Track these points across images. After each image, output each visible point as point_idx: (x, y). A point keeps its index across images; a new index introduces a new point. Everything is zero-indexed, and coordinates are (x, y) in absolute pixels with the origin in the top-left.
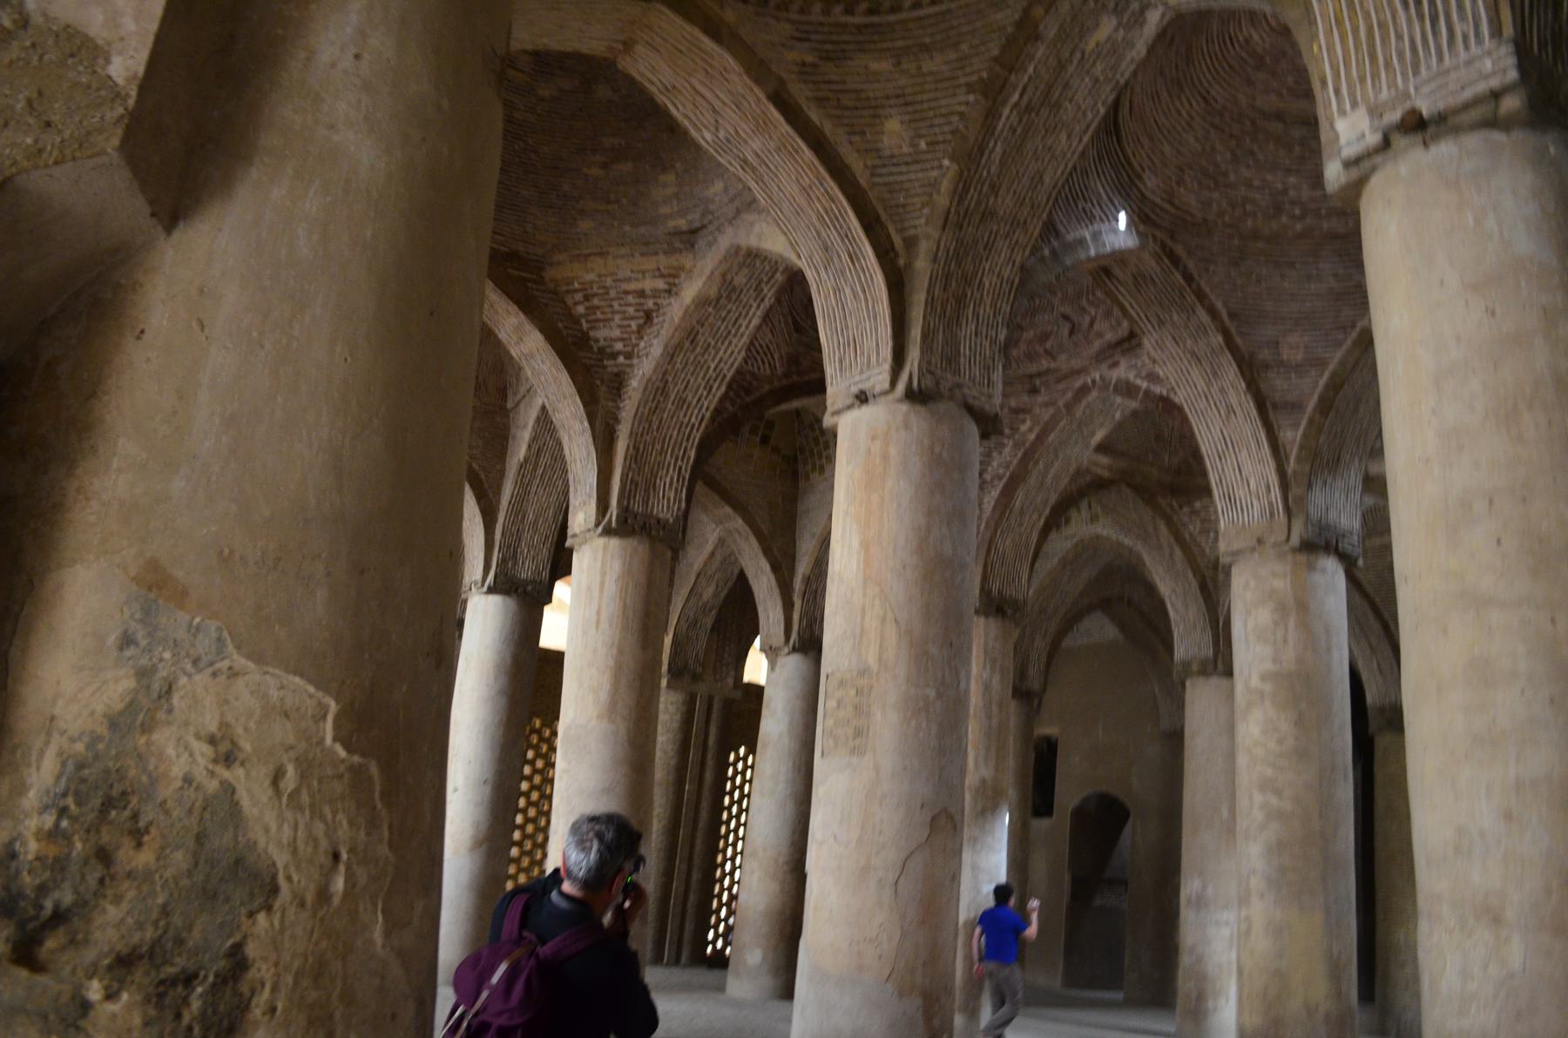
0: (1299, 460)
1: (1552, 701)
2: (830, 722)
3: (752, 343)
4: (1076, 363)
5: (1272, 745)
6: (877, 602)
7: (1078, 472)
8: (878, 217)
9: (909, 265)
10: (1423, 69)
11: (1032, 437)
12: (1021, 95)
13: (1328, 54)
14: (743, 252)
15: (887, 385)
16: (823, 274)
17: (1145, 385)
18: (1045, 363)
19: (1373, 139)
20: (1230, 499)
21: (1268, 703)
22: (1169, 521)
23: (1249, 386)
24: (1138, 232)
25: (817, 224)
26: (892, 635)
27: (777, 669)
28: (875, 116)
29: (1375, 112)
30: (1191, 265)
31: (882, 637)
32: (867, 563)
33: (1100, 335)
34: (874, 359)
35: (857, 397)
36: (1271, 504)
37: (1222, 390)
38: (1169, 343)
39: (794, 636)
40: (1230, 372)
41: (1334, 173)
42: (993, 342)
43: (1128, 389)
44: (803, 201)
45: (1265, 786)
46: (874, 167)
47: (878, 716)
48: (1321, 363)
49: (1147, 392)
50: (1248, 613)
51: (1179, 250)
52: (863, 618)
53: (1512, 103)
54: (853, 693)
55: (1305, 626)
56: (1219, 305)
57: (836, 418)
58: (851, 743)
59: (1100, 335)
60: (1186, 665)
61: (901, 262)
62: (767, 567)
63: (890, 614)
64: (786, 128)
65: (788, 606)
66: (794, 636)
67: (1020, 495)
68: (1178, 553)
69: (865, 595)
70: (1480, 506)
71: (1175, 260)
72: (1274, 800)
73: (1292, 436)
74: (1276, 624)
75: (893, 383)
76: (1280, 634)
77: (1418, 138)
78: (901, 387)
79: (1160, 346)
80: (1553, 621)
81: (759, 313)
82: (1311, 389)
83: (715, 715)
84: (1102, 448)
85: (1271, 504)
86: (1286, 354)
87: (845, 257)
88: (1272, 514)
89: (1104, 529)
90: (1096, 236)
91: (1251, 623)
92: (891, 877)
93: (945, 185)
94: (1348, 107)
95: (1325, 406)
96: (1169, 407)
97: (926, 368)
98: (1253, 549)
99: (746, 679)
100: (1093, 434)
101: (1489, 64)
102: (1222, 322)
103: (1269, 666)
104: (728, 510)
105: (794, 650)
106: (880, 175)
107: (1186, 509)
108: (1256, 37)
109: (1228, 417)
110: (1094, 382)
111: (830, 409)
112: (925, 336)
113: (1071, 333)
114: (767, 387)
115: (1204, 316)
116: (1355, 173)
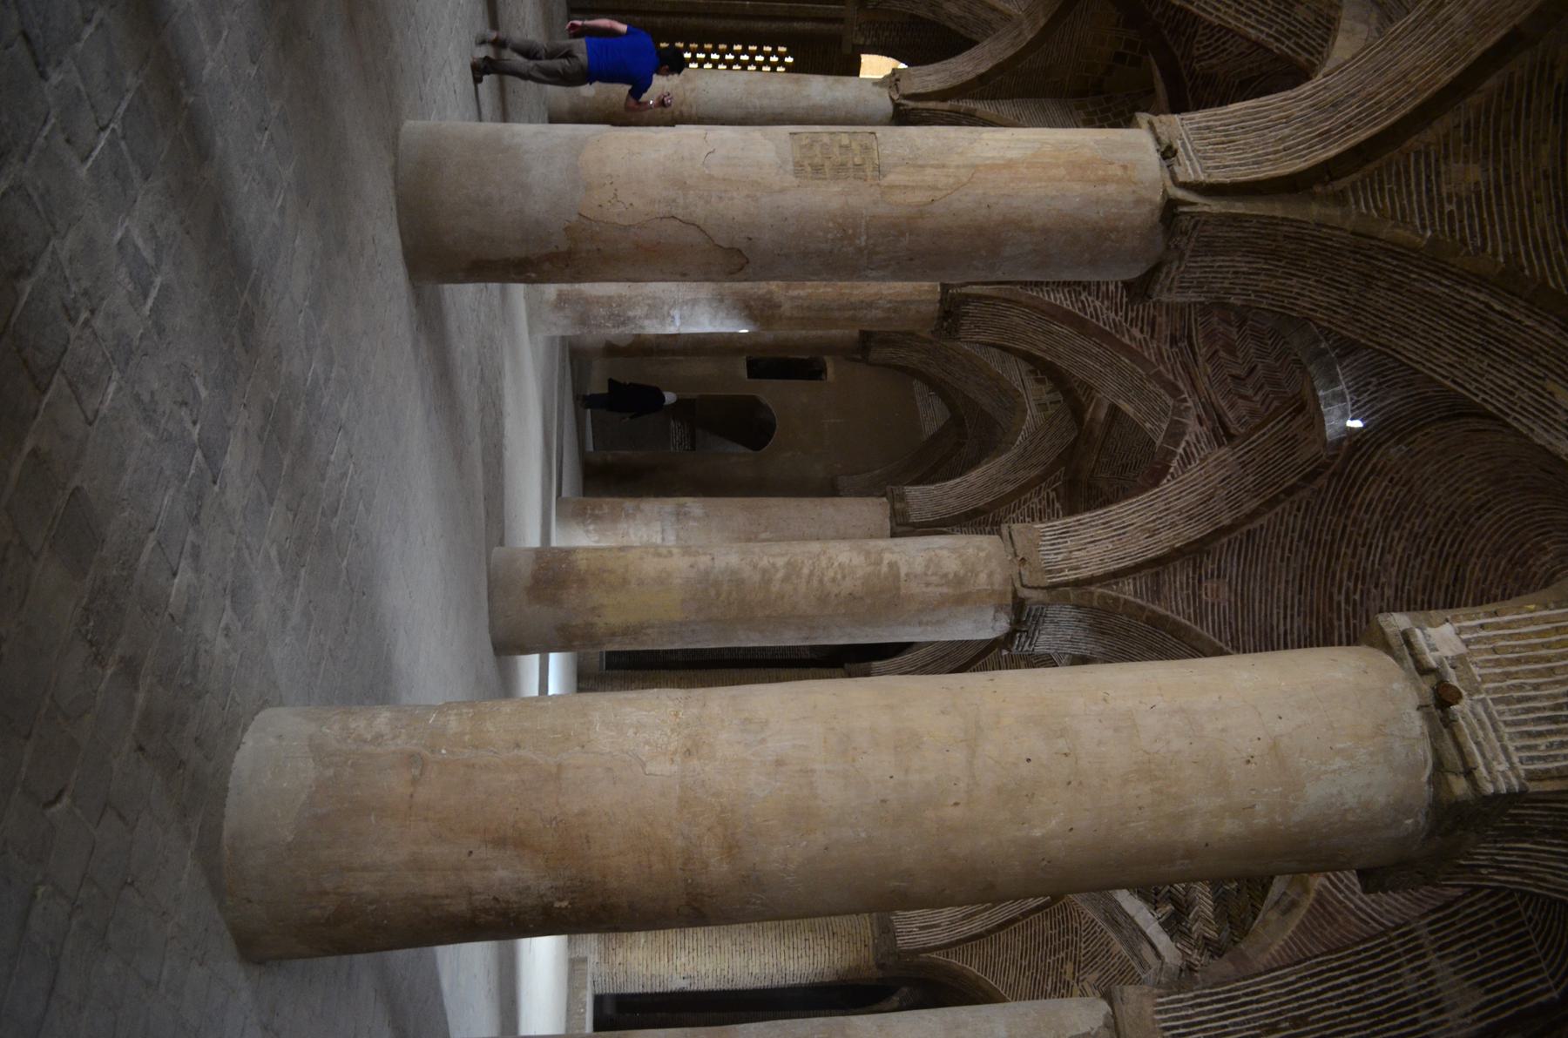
0: (1102, 596)
1: (883, 801)
2: (826, 139)
3: (1229, 31)
4: (1203, 382)
5: (831, 573)
6: (951, 180)
7: (1090, 388)
8: (1368, 161)
9: (1313, 197)
10: (1502, 707)
11: (1126, 340)
12: (1500, 313)
13: (1525, 621)
14: (1332, 13)
15: (1181, 179)
16: (1309, 102)
17: (1180, 450)
18: (1203, 351)
19: (1431, 659)
20: (1065, 533)
21: (870, 569)
22: (1042, 478)
23: (1179, 550)
24: (1341, 440)
25: (1363, 94)
26: (918, 197)
27: (877, 89)
28: (1486, 152)
29: (1459, 662)
30: (1305, 493)
31: (913, 188)
32: (993, 167)
33: (1232, 406)
34: (1210, 163)
35: (1170, 147)
36: (1062, 570)
37: (1173, 525)
38: (1223, 473)
39: (911, 104)
40: (1193, 532)
41: (1398, 621)
42: (1228, 291)
43: (1175, 434)
44: (1390, 75)
45: (793, 569)
46: (1427, 156)
47: (836, 189)
48: (1200, 617)
49: (1174, 454)
50: (954, 550)
51: (1322, 481)
52: (932, 166)
53: (1460, 786)
54: (857, 160)
55: (943, 602)
56: (1263, 520)
57: (1145, 125)
58: (806, 163)
59: (1232, 406)
60: (902, 498)
61: (1318, 189)
62: (982, 70)
63: (938, 194)
64: (1478, 50)
65: (941, 95)
66: (911, 104)
67: (1065, 330)
68: (1010, 488)
69: (958, 167)
70: (1061, 744)
71: (1309, 478)
72: (780, 575)
73: (1127, 590)
74: (946, 575)
75: (1184, 186)
76: (934, 579)
77: (1430, 701)
78: (1180, 194)
80: (956, 804)
81: (1263, 36)
82: (1174, 608)
83: (824, 27)
84: (1114, 410)
85: (1062, 570)
86: (1209, 585)
87: (1326, 126)
88: (1050, 572)
89: (1032, 417)
90: (1341, 397)
91: (945, 553)
92: (680, 212)
93: (1403, 234)
94: (1464, 637)
95: (1156, 621)
96: (1157, 475)
97: (1200, 220)
99: (865, 58)
100: (1129, 401)
101: (1501, 765)
103: (903, 571)
104: (1042, 22)
105: (896, 106)
106: (1417, 162)
107: (1052, 495)
108: (1547, 558)
109: (1149, 530)
110: (1185, 400)
111: (1155, 119)
112: (1236, 218)
113: (1234, 377)
114: (1178, 54)
116: (1396, 641)
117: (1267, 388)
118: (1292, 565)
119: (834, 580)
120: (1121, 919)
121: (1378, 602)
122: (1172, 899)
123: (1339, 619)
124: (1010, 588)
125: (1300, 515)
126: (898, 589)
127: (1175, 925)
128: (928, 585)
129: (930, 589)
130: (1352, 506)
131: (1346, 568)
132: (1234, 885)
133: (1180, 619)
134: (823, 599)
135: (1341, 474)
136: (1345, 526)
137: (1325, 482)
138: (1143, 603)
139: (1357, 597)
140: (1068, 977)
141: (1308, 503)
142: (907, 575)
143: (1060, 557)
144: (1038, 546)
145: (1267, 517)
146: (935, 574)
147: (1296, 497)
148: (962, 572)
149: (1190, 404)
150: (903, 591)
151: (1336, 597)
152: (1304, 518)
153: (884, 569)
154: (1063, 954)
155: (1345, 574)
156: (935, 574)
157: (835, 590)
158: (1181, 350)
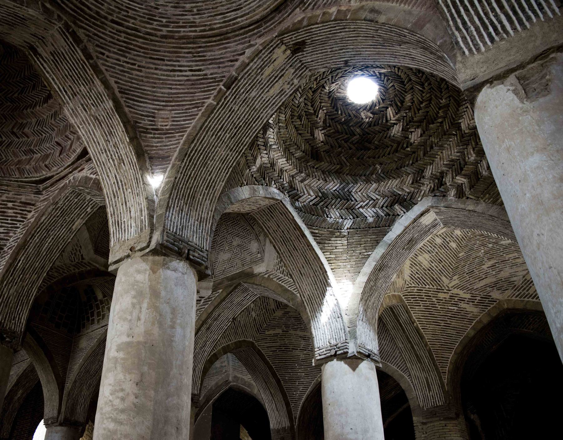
5: (117, 402)
18: (45, 174)
20: (118, 224)
21: (119, 368)
23: (130, 139)
36: (142, 221)
38: (80, 110)
48: (182, 129)
51: (81, 33)
56: (112, 81)
59: (74, 151)
74: (134, 305)
76: (135, 314)
79: (74, 113)
86: (160, 124)
88: (141, 229)
98: (128, 256)
100: (73, 221)
102: (113, 94)
103: (125, 339)
110: (70, 181)
113: (60, 154)
115: (100, 88)
117: (68, 133)
118: (143, 64)
119: (123, 399)
120: (407, 237)
121: (167, 8)
122: (391, 205)
123: (179, 32)
124: (151, 258)
125: (107, 53)
126: (139, 343)
127: (407, 203)
128: (139, 319)
129: (143, 317)
130: (97, 13)
131: (143, 25)
132: (378, 166)
133: (182, 142)
134: (138, 409)
135: (75, 17)
136: (113, 21)
137: (81, 31)
138: (170, 166)
139: (164, 20)
140: (447, 296)
141: (97, 46)
142: (128, 336)
143: (133, 224)
144: (124, 241)
145: (108, 77)
146: (131, 313)
147: (94, 55)
148: (133, 293)
149: (72, 178)
150: (141, 339)
151: (165, 33)
152: (109, 51)
153: (121, 355)
154: (434, 299)
155: (148, 26)
156: (131, 313)
157: (132, 398)
158: (44, 189)
